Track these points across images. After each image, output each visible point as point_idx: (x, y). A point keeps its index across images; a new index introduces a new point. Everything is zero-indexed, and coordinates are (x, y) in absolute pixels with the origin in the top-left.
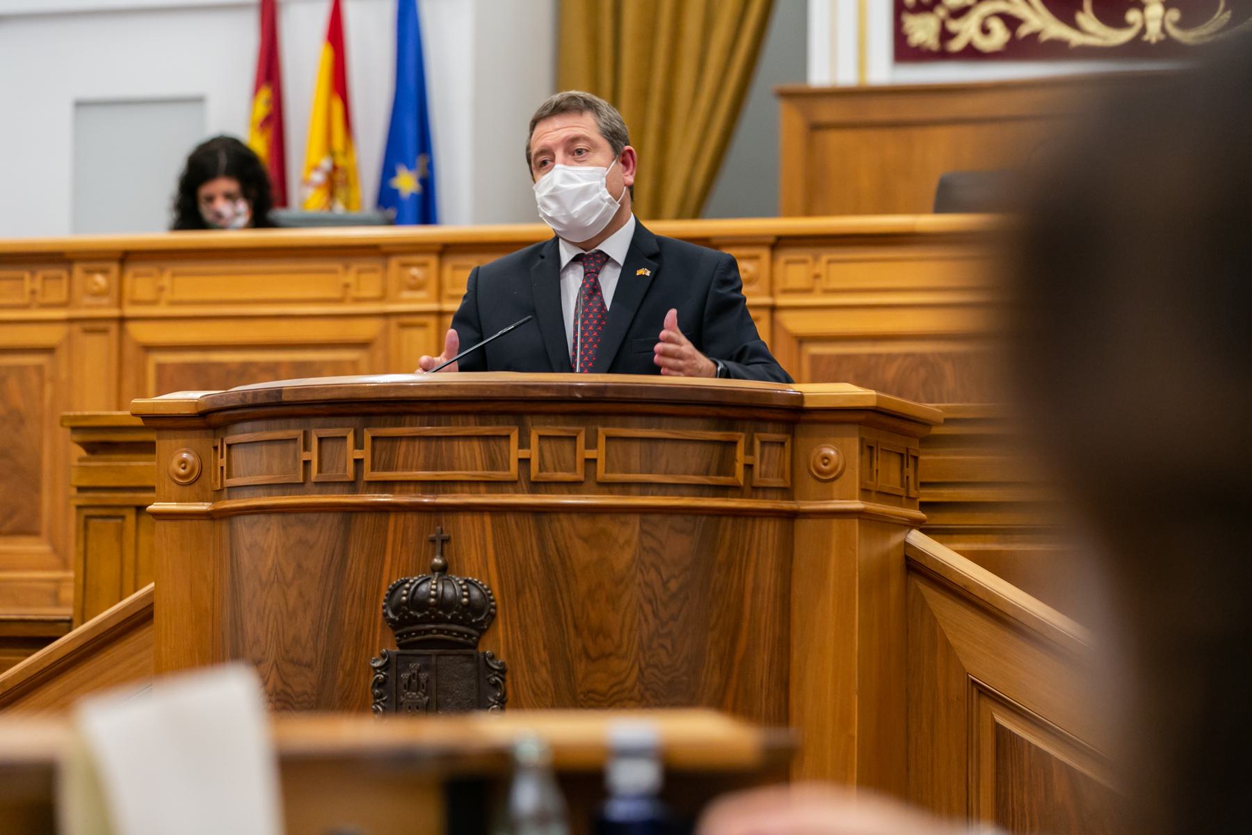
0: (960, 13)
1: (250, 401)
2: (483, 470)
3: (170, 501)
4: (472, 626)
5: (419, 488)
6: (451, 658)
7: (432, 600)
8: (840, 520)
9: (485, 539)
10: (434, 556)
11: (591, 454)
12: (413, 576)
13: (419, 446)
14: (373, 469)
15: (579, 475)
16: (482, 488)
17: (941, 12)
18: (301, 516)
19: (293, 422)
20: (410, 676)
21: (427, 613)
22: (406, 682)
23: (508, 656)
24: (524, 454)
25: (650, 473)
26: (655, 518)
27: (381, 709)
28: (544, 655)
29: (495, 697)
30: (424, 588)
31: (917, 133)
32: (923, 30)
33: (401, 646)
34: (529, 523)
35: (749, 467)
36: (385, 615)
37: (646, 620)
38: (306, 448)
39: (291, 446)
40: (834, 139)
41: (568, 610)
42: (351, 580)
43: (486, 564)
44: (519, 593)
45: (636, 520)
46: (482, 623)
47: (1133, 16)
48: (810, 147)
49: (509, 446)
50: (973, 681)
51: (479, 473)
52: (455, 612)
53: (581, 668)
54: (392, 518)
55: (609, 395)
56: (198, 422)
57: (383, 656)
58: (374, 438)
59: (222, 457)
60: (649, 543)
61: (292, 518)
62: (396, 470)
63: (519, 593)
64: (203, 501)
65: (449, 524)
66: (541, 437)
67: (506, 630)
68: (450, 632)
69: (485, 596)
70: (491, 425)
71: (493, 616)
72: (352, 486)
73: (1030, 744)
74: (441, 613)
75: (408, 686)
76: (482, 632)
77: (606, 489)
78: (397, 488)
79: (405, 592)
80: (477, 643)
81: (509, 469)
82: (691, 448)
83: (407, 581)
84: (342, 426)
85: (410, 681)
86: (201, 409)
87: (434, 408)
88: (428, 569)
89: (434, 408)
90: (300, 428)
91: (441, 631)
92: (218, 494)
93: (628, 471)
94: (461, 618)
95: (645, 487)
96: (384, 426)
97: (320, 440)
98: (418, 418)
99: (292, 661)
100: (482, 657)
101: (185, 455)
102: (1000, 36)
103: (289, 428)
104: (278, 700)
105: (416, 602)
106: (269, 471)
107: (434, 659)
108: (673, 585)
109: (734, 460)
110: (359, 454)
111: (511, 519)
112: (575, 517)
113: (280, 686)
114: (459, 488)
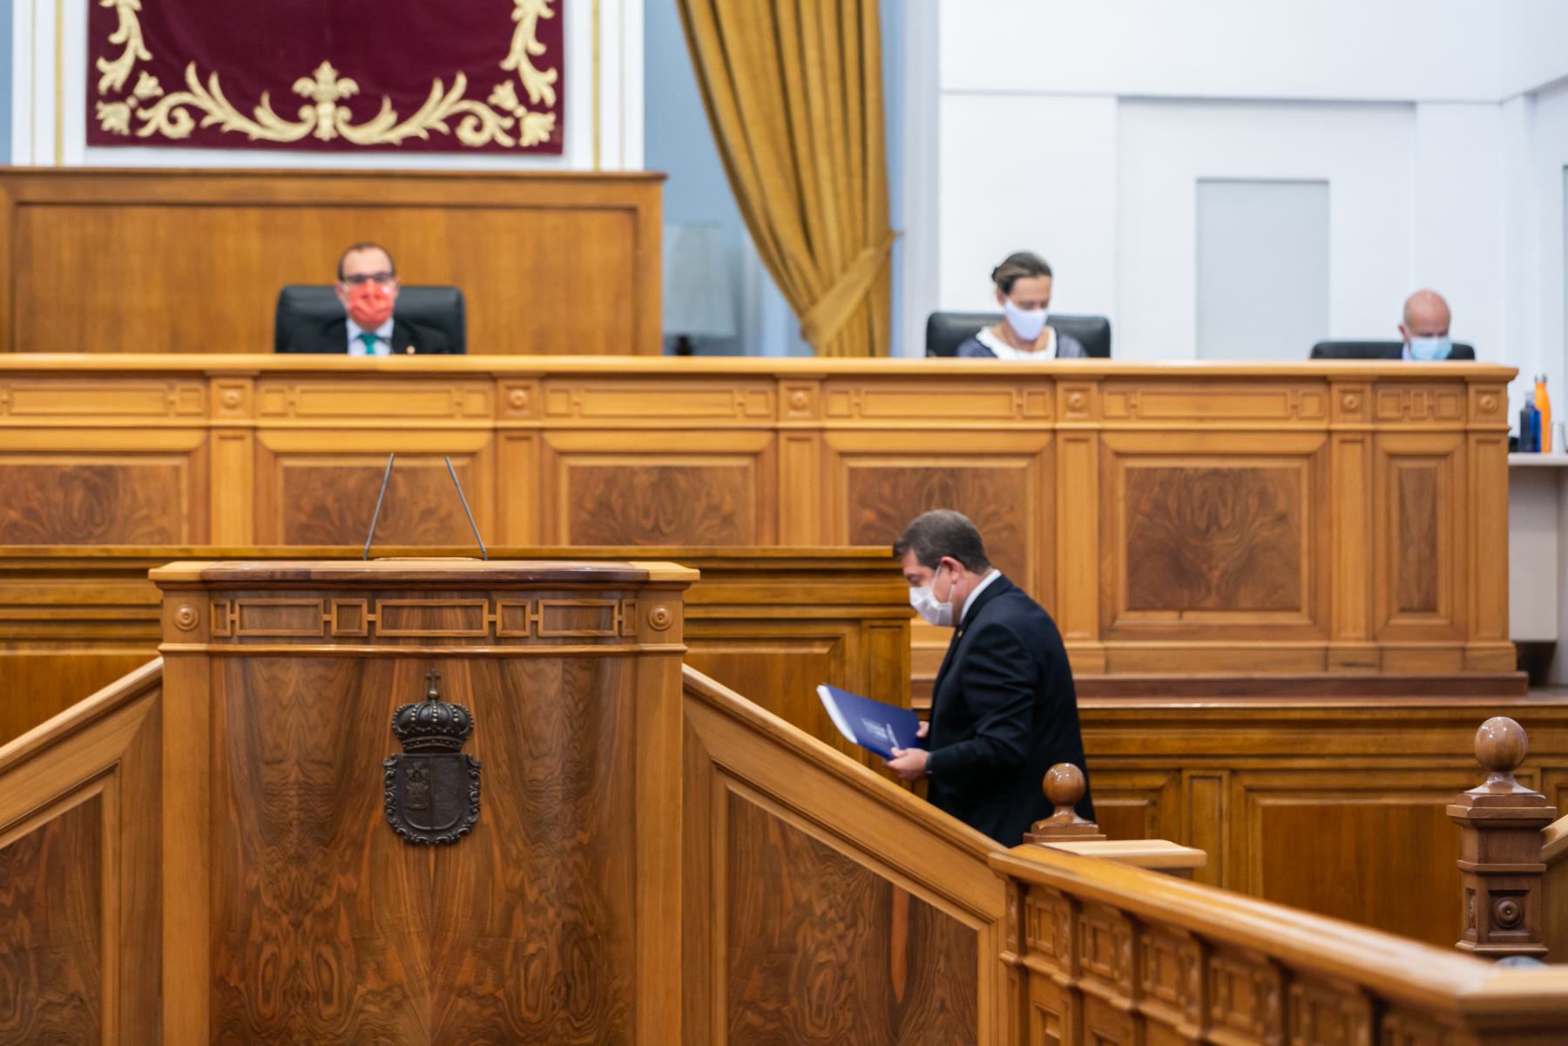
0: (150, 103)
1: (278, 577)
2: (464, 629)
3: (173, 641)
4: (459, 737)
5: (417, 641)
6: (442, 759)
7: (435, 720)
8: (670, 658)
9: (465, 677)
10: (430, 688)
11: (534, 618)
12: (417, 702)
13: (417, 612)
14: (383, 628)
15: (527, 633)
16: (463, 642)
17: (132, 101)
18: (321, 659)
19: (312, 593)
20: (414, 773)
21: (429, 728)
22: (411, 776)
23: (481, 756)
24: (492, 618)
25: (568, 629)
26: (571, 660)
27: (392, 794)
28: (505, 755)
29: (474, 786)
30: (425, 712)
31: (115, 211)
32: (115, 117)
33: (406, 751)
34: (495, 665)
35: (620, 623)
36: (394, 730)
37: (567, 731)
38: (327, 611)
39: (311, 610)
40: (37, 214)
41: (520, 726)
42: (365, 705)
43: (466, 695)
44: (488, 714)
45: (559, 662)
46: (464, 735)
47: (306, 112)
48: (15, 221)
49: (482, 612)
50: (715, 763)
51: (461, 631)
52: (449, 728)
53: (528, 764)
54: (397, 663)
55: (549, 577)
56: (201, 586)
57: (393, 758)
58: (384, 607)
59: (232, 611)
60: (569, 678)
61: (311, 661)
62: (400, 628)
63: (488, 714)
64: (200, 642)
65: (438, 667)
66: (504, 606)
67: (480, 739)
68: (444, 741)
69: (467, 716)
70: (468, 598)
71: (471, 729)
72: (365, 640)
73: (752, 805)
74: (439, 728)
75: (413, 779)
76: (465, 740)
77: (542, 641)
78: (401, 641)
79: (413, 714)
80: (461, 748)
81: (481, 628)
82: (590, 612)
83: (412, 706)
84: (356, 597)
85: (414, 776)
86: (207, 578)
87: (430, 586)
88: (425, 696)
89: (430, 586)
90: (319, 597)
91: (438, 741)
92: (226, 639)
93: (556, 629)
94: (453, 731)
95: (567, 640)
96: (391, 598)
97: (339, 606)
98: (417, 594)
99: (313, 761)
100: (465, 759)
101: (184, 610)
102: (185, 125)
103: (308, 597)
104: (300, 788)
105: (421, 722)
106: (289, 626)
107: (431, 761)
108: (581, 706)
109: (612, 618)
110: (371, 617)
111: (483, 663)
112: (523, 660)
113: (302, 778)
114: (446, 642)
